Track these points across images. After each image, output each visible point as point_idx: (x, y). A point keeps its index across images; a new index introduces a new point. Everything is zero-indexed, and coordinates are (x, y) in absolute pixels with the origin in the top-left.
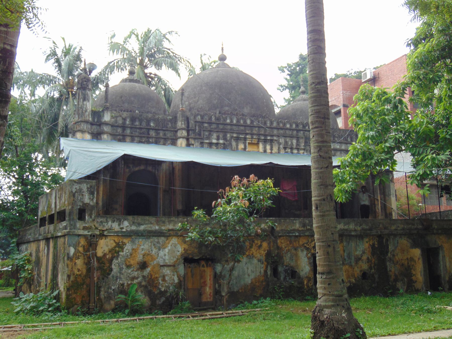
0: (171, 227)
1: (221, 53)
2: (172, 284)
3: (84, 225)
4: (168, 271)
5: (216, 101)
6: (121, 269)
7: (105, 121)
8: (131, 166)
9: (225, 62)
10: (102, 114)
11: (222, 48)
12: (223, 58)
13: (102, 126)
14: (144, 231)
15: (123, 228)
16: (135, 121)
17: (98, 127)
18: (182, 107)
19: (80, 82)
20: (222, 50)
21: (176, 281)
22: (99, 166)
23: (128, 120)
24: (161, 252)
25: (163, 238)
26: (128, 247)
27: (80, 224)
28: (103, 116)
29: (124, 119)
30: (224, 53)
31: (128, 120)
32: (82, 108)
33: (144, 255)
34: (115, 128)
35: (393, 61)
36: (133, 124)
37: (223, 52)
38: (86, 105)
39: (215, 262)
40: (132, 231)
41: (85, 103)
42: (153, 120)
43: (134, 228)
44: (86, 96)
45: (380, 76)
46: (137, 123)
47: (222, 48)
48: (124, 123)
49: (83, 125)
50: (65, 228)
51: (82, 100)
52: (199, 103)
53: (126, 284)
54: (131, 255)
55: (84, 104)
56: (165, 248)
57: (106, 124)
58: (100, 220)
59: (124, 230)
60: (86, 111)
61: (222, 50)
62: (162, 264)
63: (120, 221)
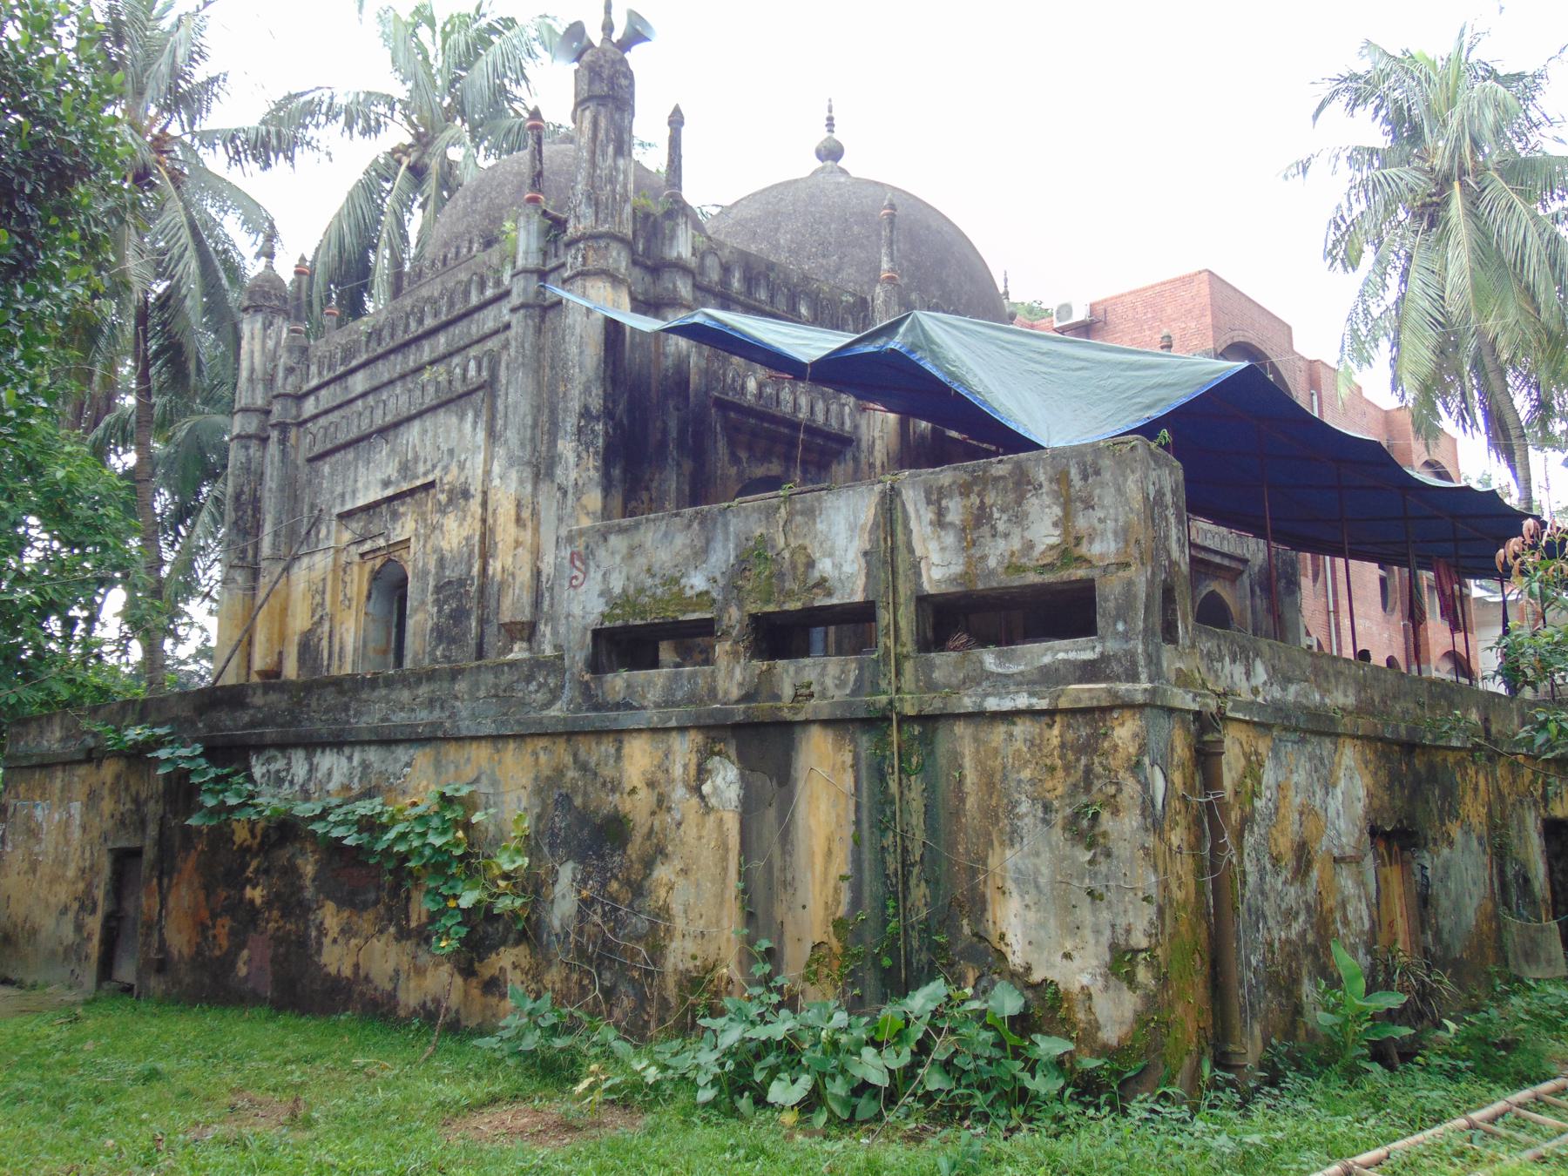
0: (1341, 700)
1: (827, 135)
2: (1362, 932)
3: (1178, 665)
4: (1350, 883)
5: (906, 280)
6: (1262, 872)
7: (679, 257)
8: (743, 455)
9: (841, 163)
10: (668, 224)
11: (830, 119)
12: (831, 152)
13: (666, 276)
14: (1298, 706)
15: (1255, 691)
16: (758, 285)
17: (648, 279)
18: (892, 270)
19: (606, 73)
20: (830, 123)
21: (1367, 925)
22: (1146, 399)
23: (737, 275)
24: (1329, 799)
25: (1328, 744)
26: (1269, 776)
27: (1171, 661)
28: (673, 237)
29: (726, 269)
30: (836, 136)
31: (737, 275)
32: (611, 180)
33: (1301, 813)
34: (698, 294)
35: (1164, 283)
36: (749, 293)
37: (831, 131)
38: (626, 176)
39: (1415, 845)
40: (1278, 708)
41: (621, 163)
42: (807, 294)
43: (1276, 692)
44: (626, 137)
45: (1110, 317)
46: (762, 295)
47: (830, 119)
48: (725, 282)
49: (614, 254)
50: (1089, 671)
51: (611, 149)
52: (842, 275)
53: (1277, 944)
54: (1277, 809)
55: (616, 169)
56: (1335, 786)
57: (679, 266)
58: (1207, 645)
59: (1260, 699)
60: (625, 199)
61: (830, 123)
62: (1336, 852)
63: (1247, 658)
